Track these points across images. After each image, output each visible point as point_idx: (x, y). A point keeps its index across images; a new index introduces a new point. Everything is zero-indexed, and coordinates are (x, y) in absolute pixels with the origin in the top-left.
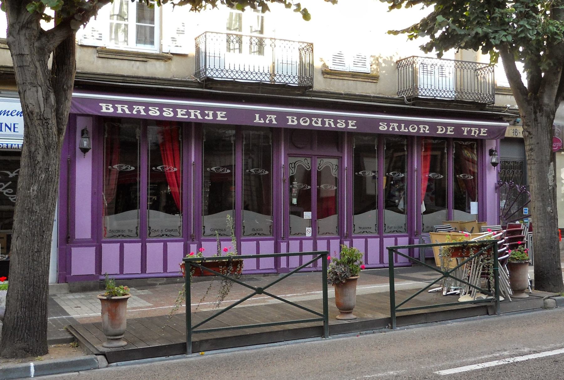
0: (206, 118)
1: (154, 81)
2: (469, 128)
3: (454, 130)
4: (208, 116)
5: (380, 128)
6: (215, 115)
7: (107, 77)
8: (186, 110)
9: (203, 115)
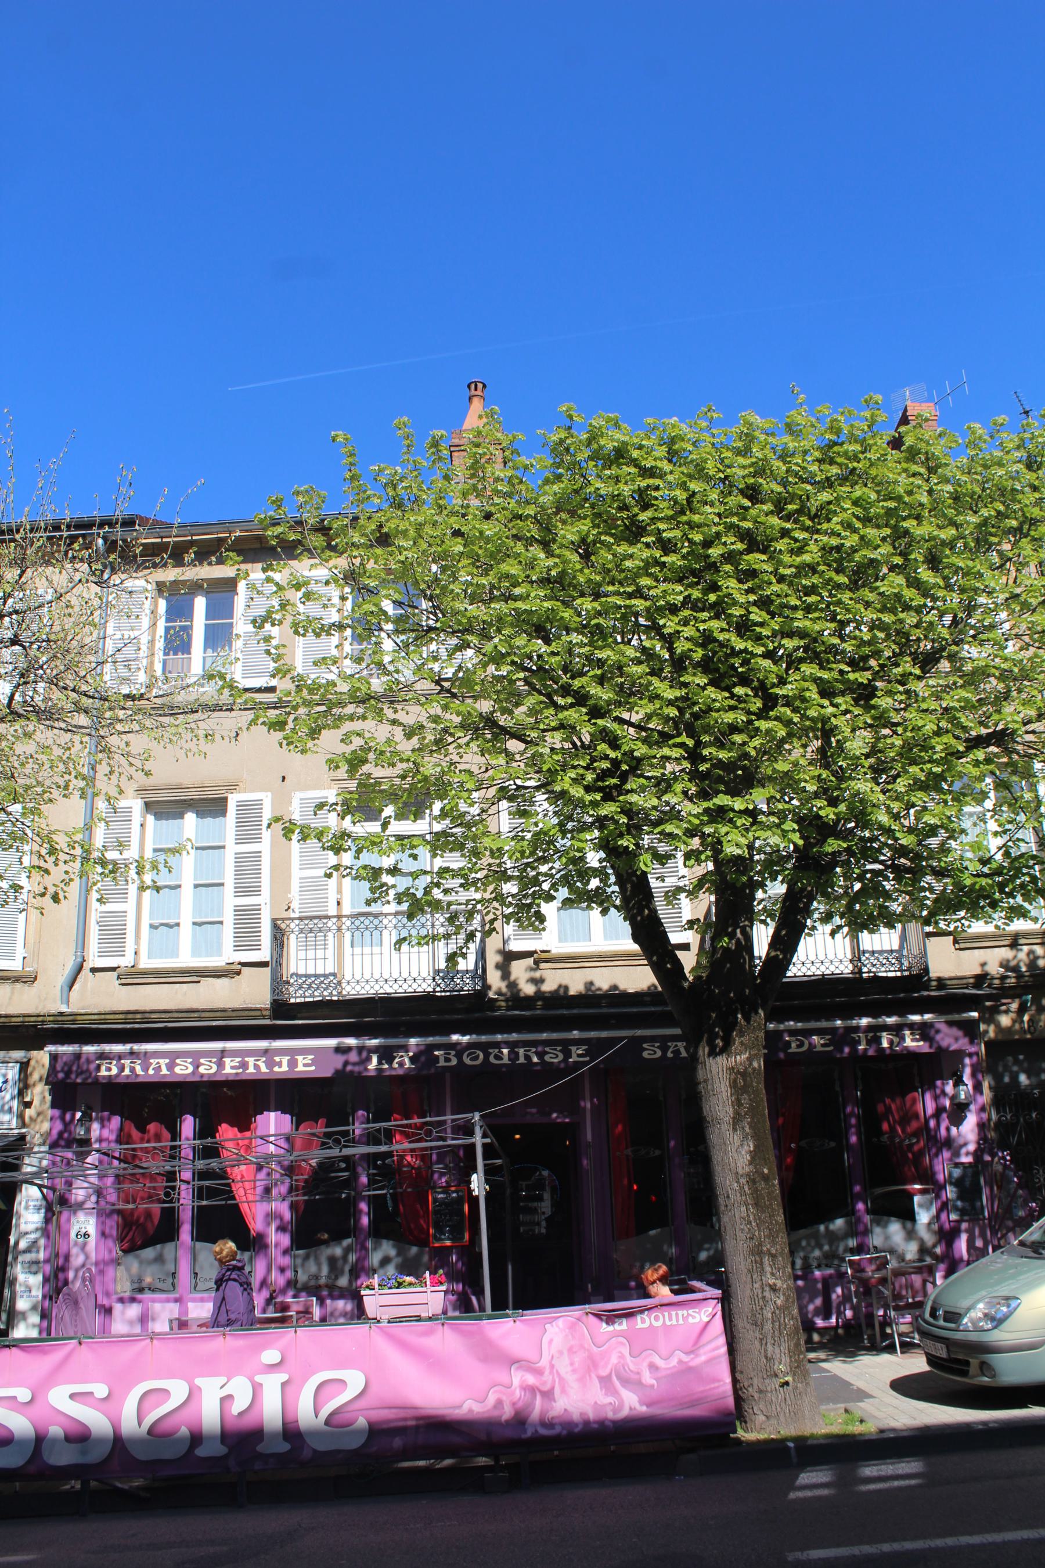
0: (276, 1069)
1: (196, 1015)
2: (871, 1035)
3: (314, 1062)
4: (280, 1066)
5: (645, 1054)
6: (293, 1063)
7: (112, 1017)
8: (239, 1059)
9: (270, 1064)
